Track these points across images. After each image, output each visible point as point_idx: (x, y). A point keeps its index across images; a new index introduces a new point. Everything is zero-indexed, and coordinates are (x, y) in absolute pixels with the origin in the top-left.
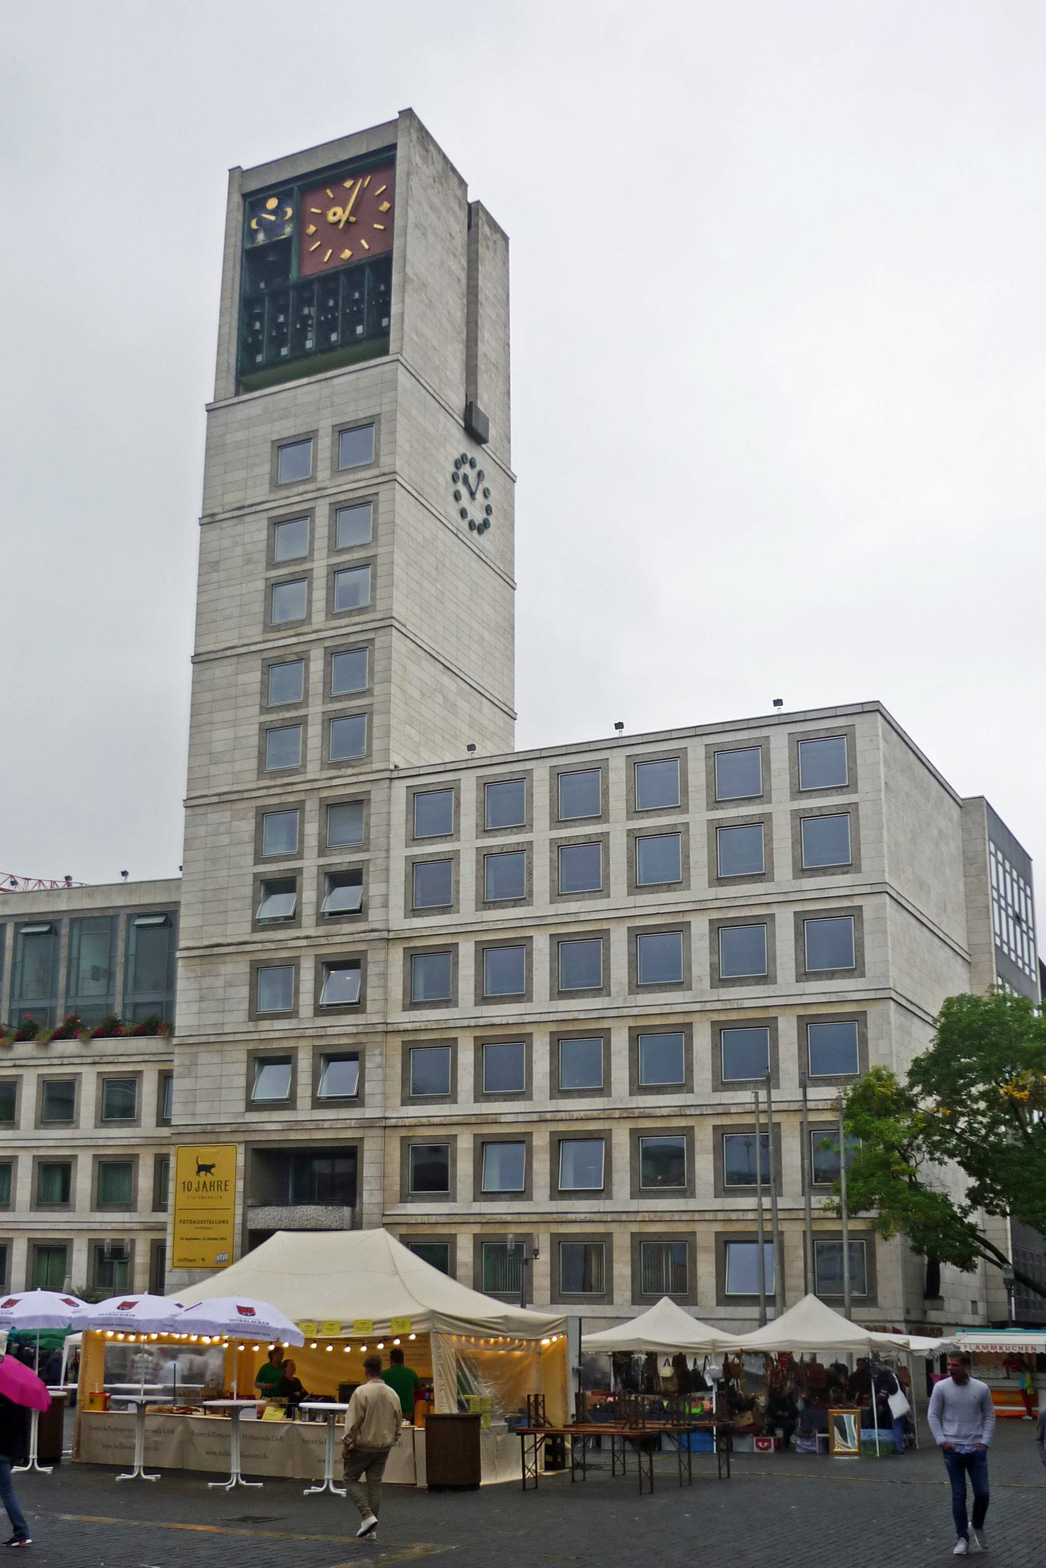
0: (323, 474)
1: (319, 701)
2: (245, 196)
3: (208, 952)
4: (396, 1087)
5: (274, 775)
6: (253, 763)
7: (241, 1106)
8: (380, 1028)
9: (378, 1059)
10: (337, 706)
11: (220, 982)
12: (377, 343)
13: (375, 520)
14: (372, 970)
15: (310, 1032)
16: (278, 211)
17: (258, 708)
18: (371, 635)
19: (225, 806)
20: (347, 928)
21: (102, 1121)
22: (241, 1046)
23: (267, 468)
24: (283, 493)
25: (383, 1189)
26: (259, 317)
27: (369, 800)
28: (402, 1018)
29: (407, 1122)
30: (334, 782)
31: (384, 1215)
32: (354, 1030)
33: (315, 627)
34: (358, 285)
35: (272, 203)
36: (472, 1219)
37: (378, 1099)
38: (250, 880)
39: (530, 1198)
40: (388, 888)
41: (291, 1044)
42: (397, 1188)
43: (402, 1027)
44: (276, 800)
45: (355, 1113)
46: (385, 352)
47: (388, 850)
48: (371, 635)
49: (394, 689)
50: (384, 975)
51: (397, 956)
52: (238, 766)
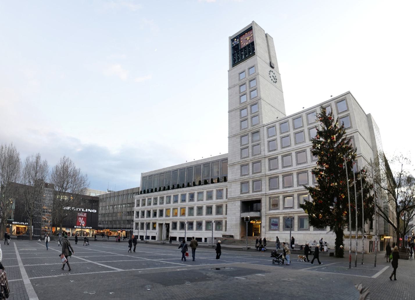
1: (250, 114)
4: (268, 187)
5: (243, 129)
7: (240, 193)
8: (265, 175)
9: (264, 181)
10: (253, 115)
11: (235, 170)
14: (263, 164)
15: (251, 178)
17: (239, 118)
19: (234, 137)
20: (257, 156)
21: (217, 198)
25: (266, 208)
27: (260, 131)
28: (268, 173)
29: (270, 194)
30: (253, 129)
31: (266, 213)
32: (260, 176)
36: (283, 213)
38: (240, 149)
39: (294, 208)
40: (264, 147)
42: (268, 208)
44: (243, 134)
47: (264, 140)
48: (258, 101)
49: (262, 110)
50: (265, 165)
51: (267, 160)
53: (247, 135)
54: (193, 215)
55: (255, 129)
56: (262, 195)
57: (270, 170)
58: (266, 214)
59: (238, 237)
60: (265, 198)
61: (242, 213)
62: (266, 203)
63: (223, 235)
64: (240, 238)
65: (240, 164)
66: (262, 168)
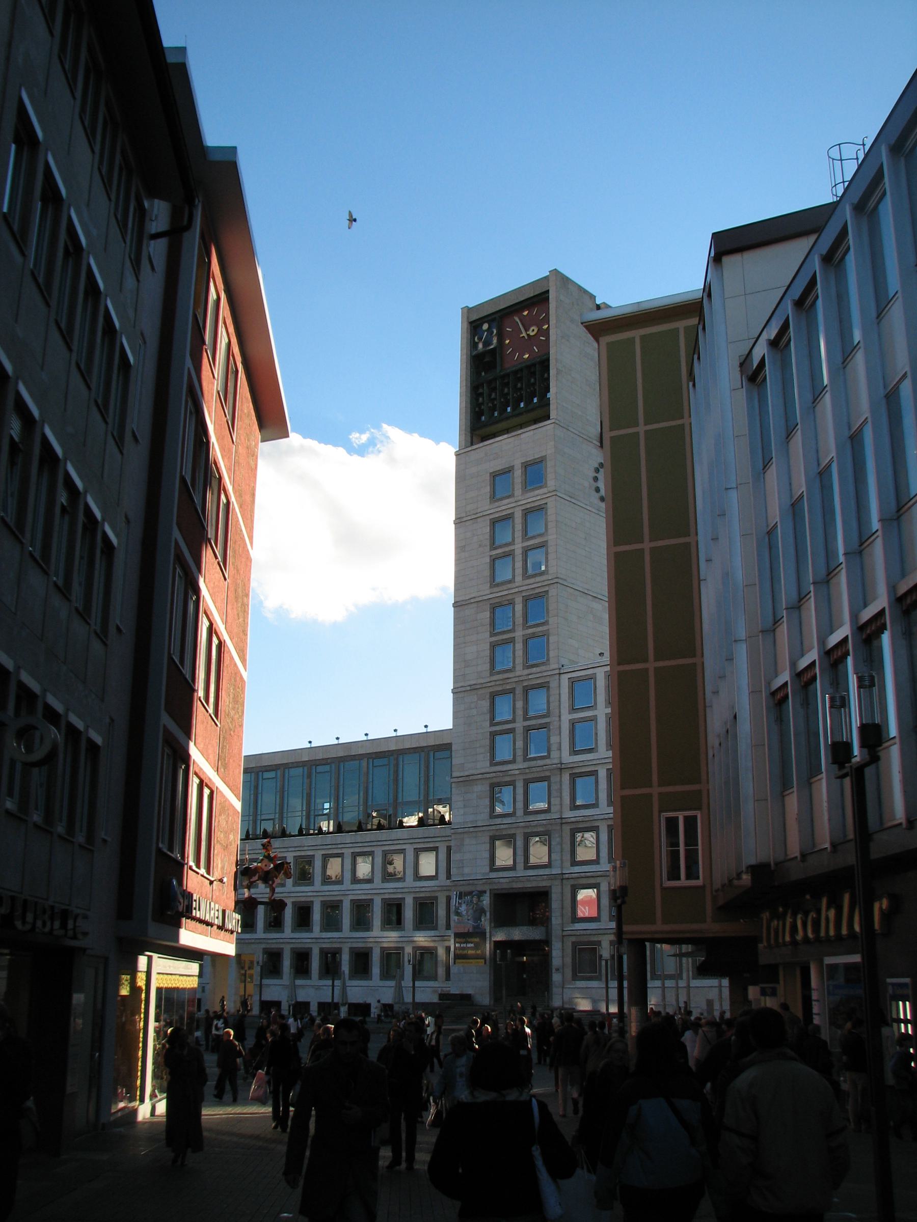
0: (518, 491)
2: (471, 323)
3: (467, 779)
4: (567, 857)
5: (499, 673)
6: (487, 666)
9: (558, 839)
10: (531, 631)
12: (541, 414)
13: (546, 519)
14: (554, 787)
16: (489, 330)
18: (546, 589)
23: (488, 489)
24: (497, 504)
25: (562, 916)
26: (481, 394)
30: (530, 677)
33: (517, 584)
34: (533, 374)
35: (485, 326)
37: (558, 863)
41: (513, 832)
43: (569, 820)
44: (500, 688)
45: (546, 871)
46: (548, 418)
47: (560, 717)
51: (566, 778)
53: (512, 691)
54: (339, 929)
55: (535, 675)
56: (552, 877)
57: (574, 807)
58: (565, 933)
59: (485, 1000)
60: (560, 887)
61: (495, 927)
62: (562, 901)
63: (440, 995)
64: (492, 1003)
65: (488, 782)
66: (552, 800)
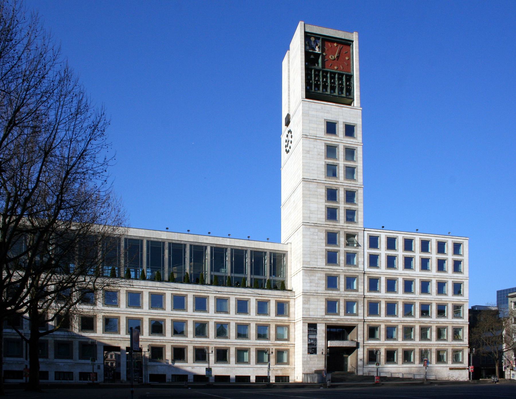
3: (313, 269)
11: (317, 278)
22: (323, 297)
41: (338, 298)
45: (356, 317)
52: (319, 216)
56: (359, 320)
